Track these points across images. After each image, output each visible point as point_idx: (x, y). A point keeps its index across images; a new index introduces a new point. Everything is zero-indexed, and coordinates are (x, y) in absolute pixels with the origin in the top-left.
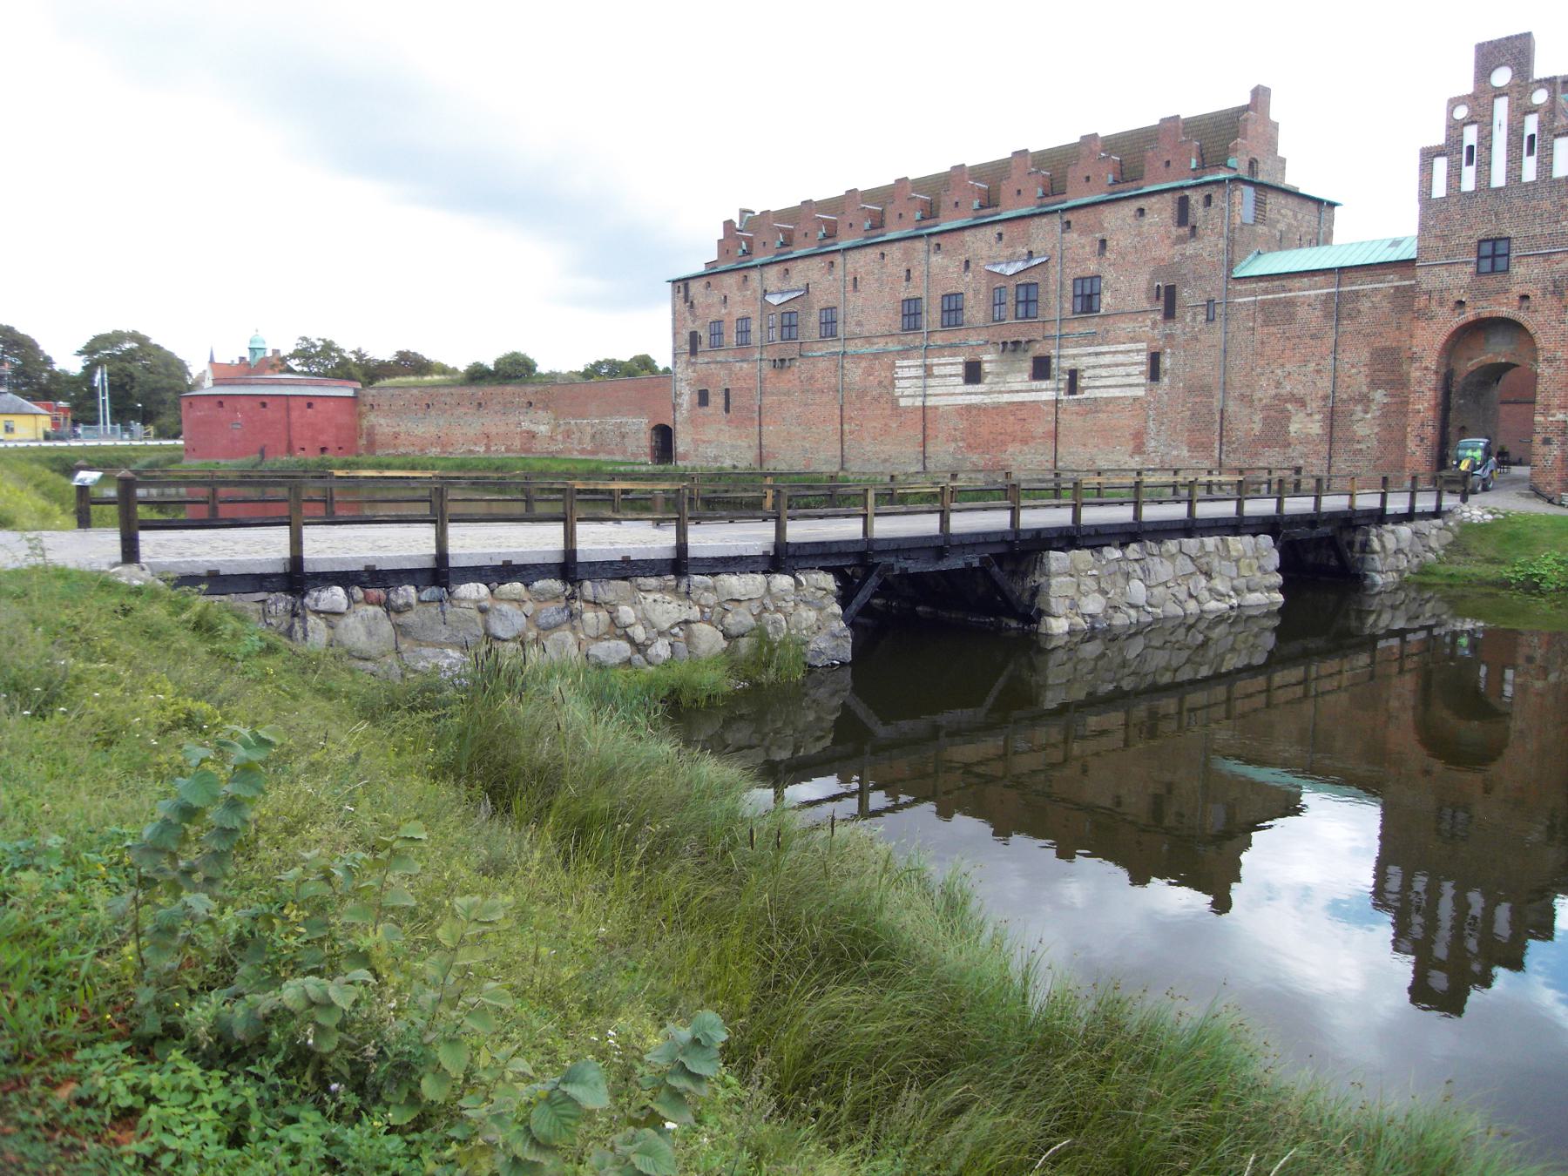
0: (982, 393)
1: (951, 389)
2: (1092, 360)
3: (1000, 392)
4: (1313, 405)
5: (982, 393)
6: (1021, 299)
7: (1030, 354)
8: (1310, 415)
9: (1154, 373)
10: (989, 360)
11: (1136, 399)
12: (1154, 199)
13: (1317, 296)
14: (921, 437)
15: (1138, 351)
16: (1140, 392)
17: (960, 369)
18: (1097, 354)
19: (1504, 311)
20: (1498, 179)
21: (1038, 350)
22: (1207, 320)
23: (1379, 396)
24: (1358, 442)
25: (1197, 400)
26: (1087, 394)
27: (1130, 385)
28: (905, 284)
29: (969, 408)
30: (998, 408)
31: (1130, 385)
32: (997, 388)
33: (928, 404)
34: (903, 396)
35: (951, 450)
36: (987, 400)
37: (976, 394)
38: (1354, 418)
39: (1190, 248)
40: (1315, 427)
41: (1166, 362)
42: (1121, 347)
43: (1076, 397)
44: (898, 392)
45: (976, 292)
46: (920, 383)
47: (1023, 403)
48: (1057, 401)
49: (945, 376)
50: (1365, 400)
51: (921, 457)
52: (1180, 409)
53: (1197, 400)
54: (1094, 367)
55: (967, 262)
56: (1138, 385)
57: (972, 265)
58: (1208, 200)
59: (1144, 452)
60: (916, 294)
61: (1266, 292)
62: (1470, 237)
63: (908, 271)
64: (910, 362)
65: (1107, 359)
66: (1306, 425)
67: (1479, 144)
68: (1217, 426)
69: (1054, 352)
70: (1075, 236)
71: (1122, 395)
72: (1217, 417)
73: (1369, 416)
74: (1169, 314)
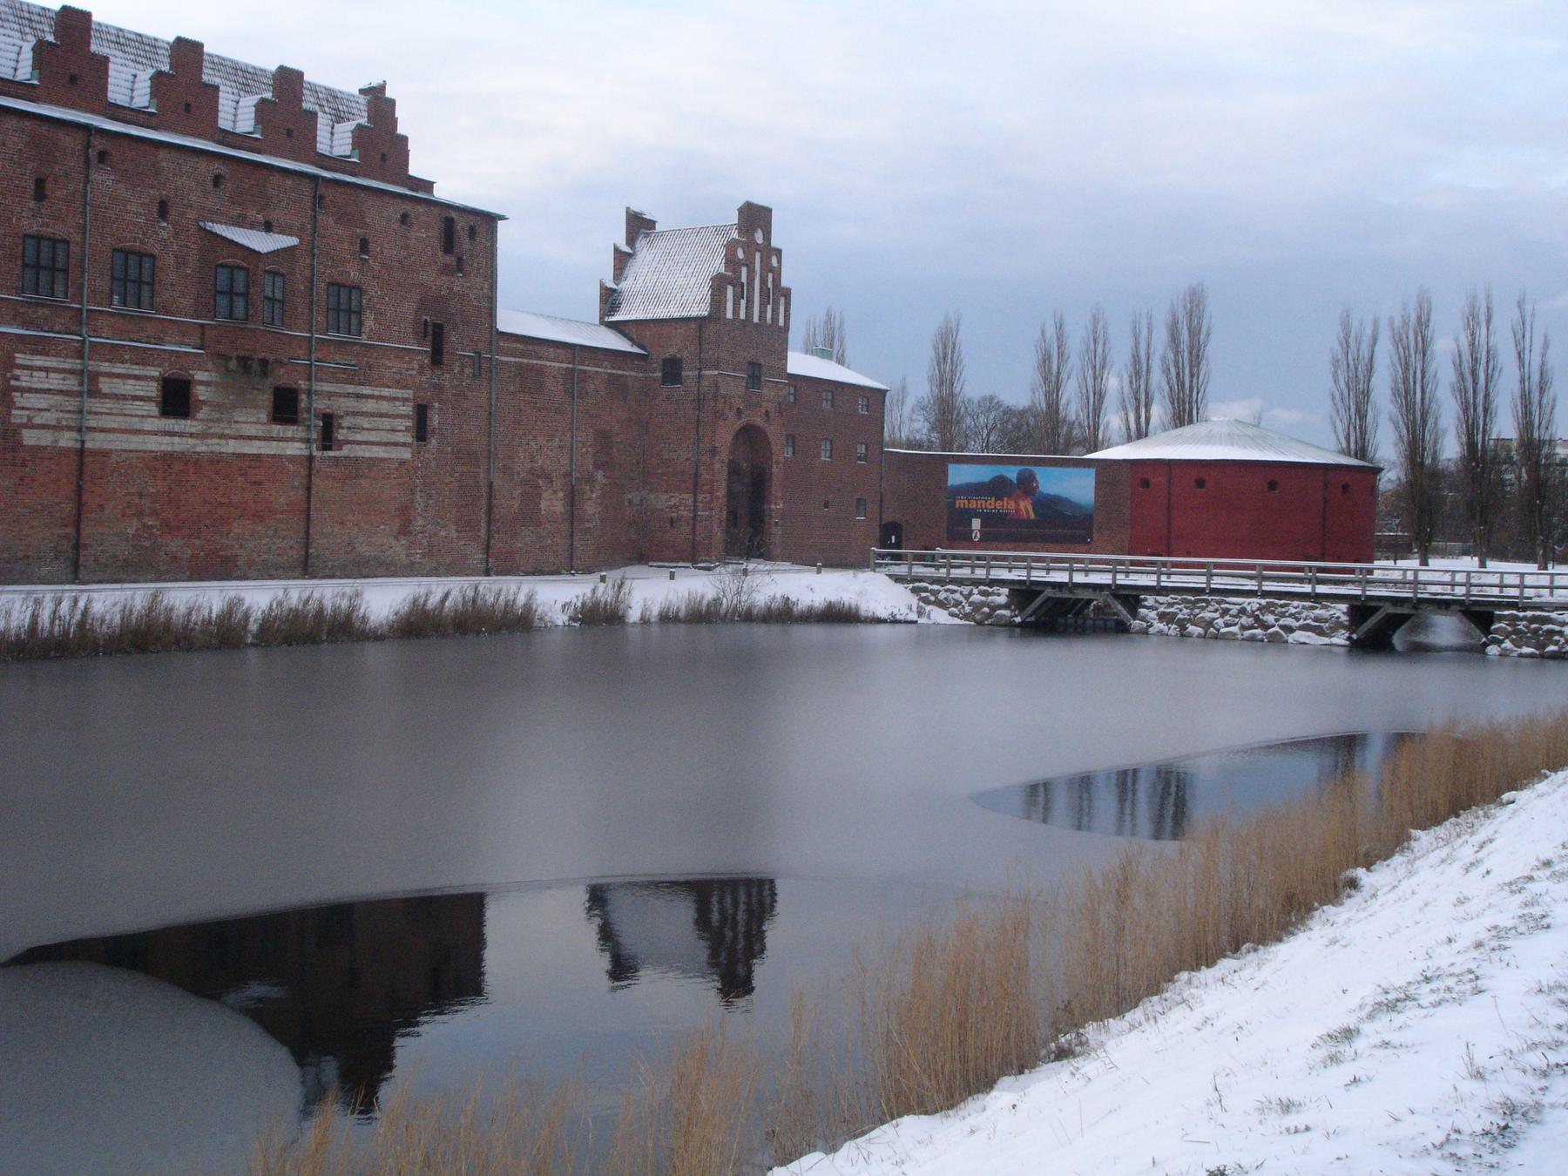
0: (192, 435)
1: (136, 423)
2: (350, 404)
3: (222, 436)
4: (558, 483)
5: (192, 435)
6: (343, 307)
7: (269, 382)
8: (555, 492)
9: (421, 431)
10: (205, 382)
11: (402, 463)
12: (421, 209)
13: (559, 368)
14: (69, 507)
15: (405, 400)
16: (406, 454)
17: (153, 389)
18: (358, 396)
19: (759, 421)
20: (756, 320)
21: (283, 377)
22: (474, 375)
23: (600, 476)
24: (588, 521)
25: (464, 468)
26: (346, 451)
27: (396, 444)
28: (32, 204)
29: (168, 458)
30: (217, 459)
31: (396, 444)
32: (217, 429)
33: (88, 445)
34: (26, 426)
35: (131, 531)
36: (202, 448)
37: (181, 435)
38: (585, 498)
39: (459, 283)
40: (559, 507)
41: (435, 420)
42: (386, 392)
43: (331, 454)
44: (18, 416)
45: (181, 262)
46: (71, 404)
47: (258, 457)
48: (310, 458)
49: (124, 397)
50: (590, 479)
51: (66, 546)
52: (448, 479)
53: (464, 468)
54: (354, 414)
55: (163, 208)
56: (404, 445)
57: (173, 214)
58: (472, 233)
59: (410, 533)
60: (60, 230)
61: (523, 355)
62: (744, 358)
63: (40, 183)
64: (50, 362)
65: (370, 406)
66: (552, 503)
67: (748, 283)
68: (483, 502)
69: (303, 384)
70: (331, 221)
71: (386, 456)
72: (484, 491)
73: (594, 496)
74: (437, 357)
